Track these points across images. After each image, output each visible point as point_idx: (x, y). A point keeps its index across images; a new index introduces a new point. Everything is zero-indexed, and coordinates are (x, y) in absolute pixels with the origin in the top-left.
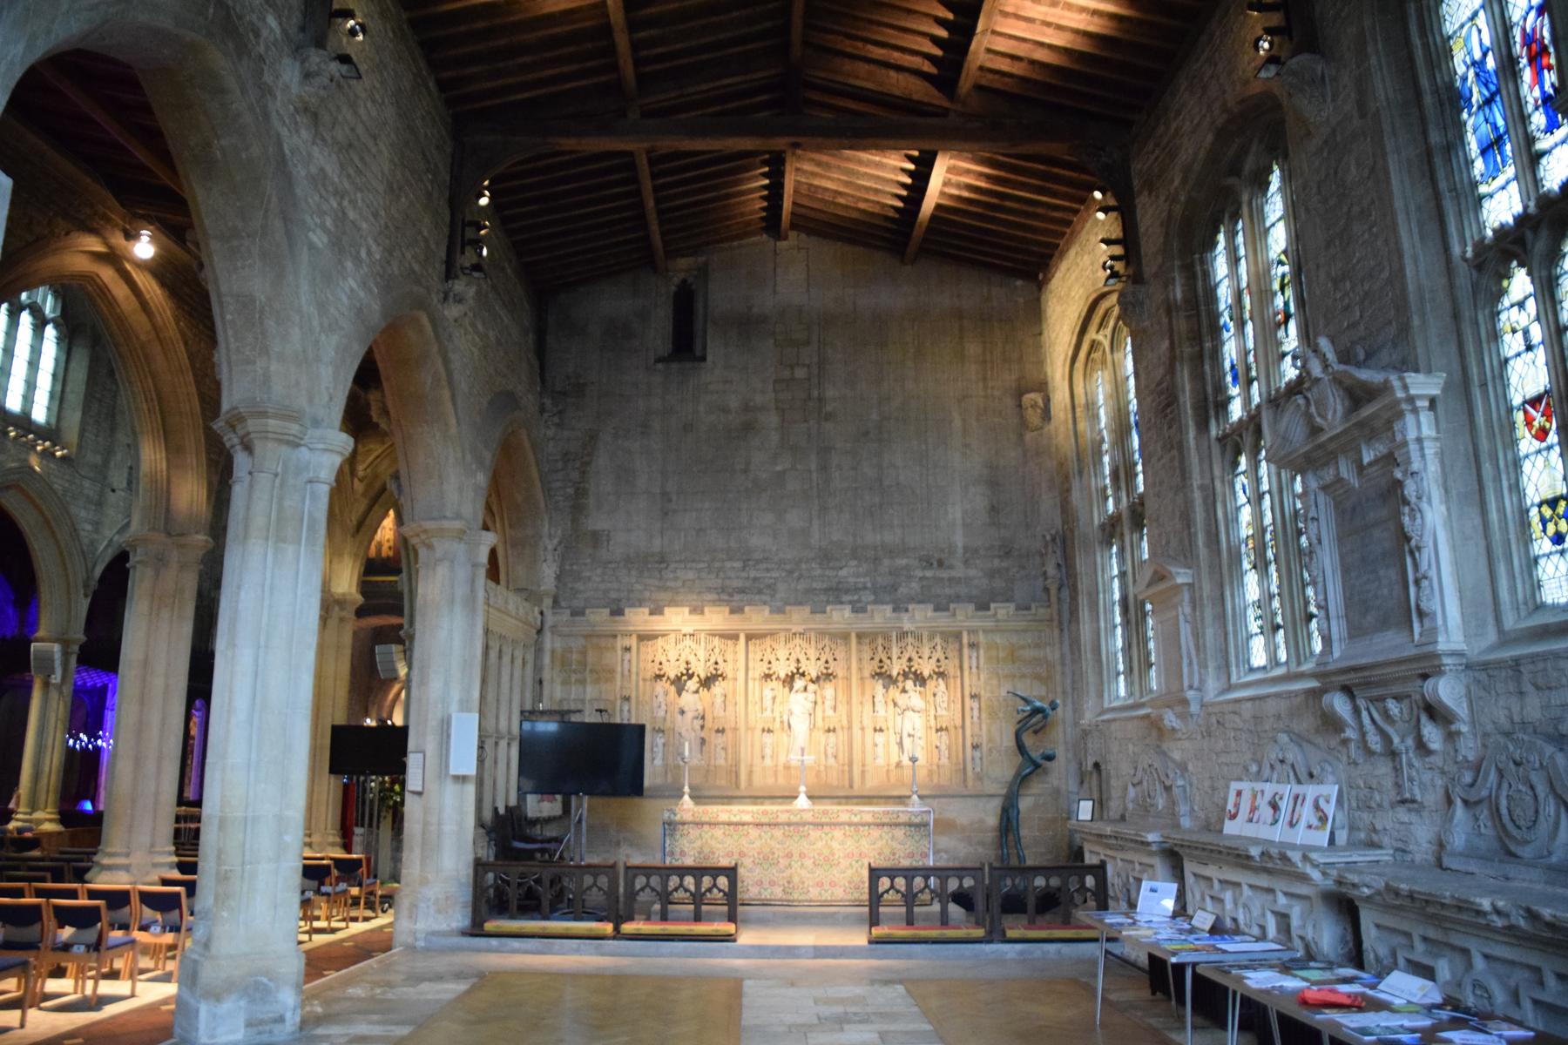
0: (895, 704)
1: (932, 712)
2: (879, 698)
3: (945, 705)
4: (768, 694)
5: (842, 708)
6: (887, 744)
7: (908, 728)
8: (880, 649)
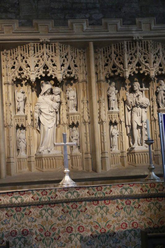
0: (126, 102)
2: (113, 97)
4: (20, 96)
5: (85, 108)
6: (121, 134)
7: (137, 120)
8: (113, 56)
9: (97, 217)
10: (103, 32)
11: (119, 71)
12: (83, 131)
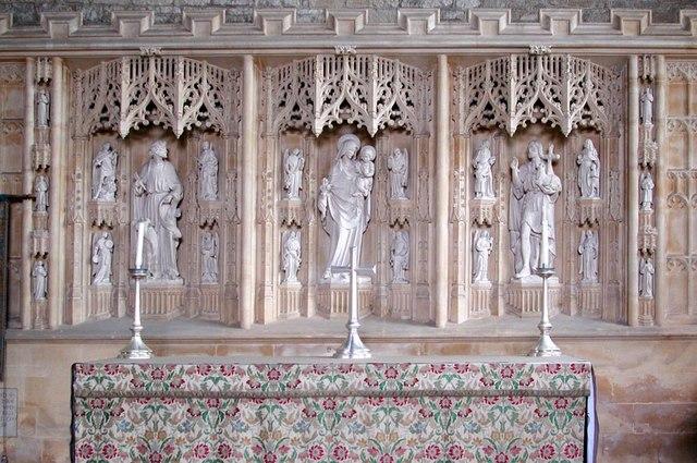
1: (572, 199)
2: (484, 170)
3: (596, 183)
4: (294, 161)
8: (488, 86)
9: (375, 430)
10: (466, 37)
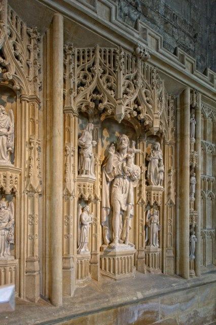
2: (89, 151)
11: (106, 103)
12: (26, 210)
